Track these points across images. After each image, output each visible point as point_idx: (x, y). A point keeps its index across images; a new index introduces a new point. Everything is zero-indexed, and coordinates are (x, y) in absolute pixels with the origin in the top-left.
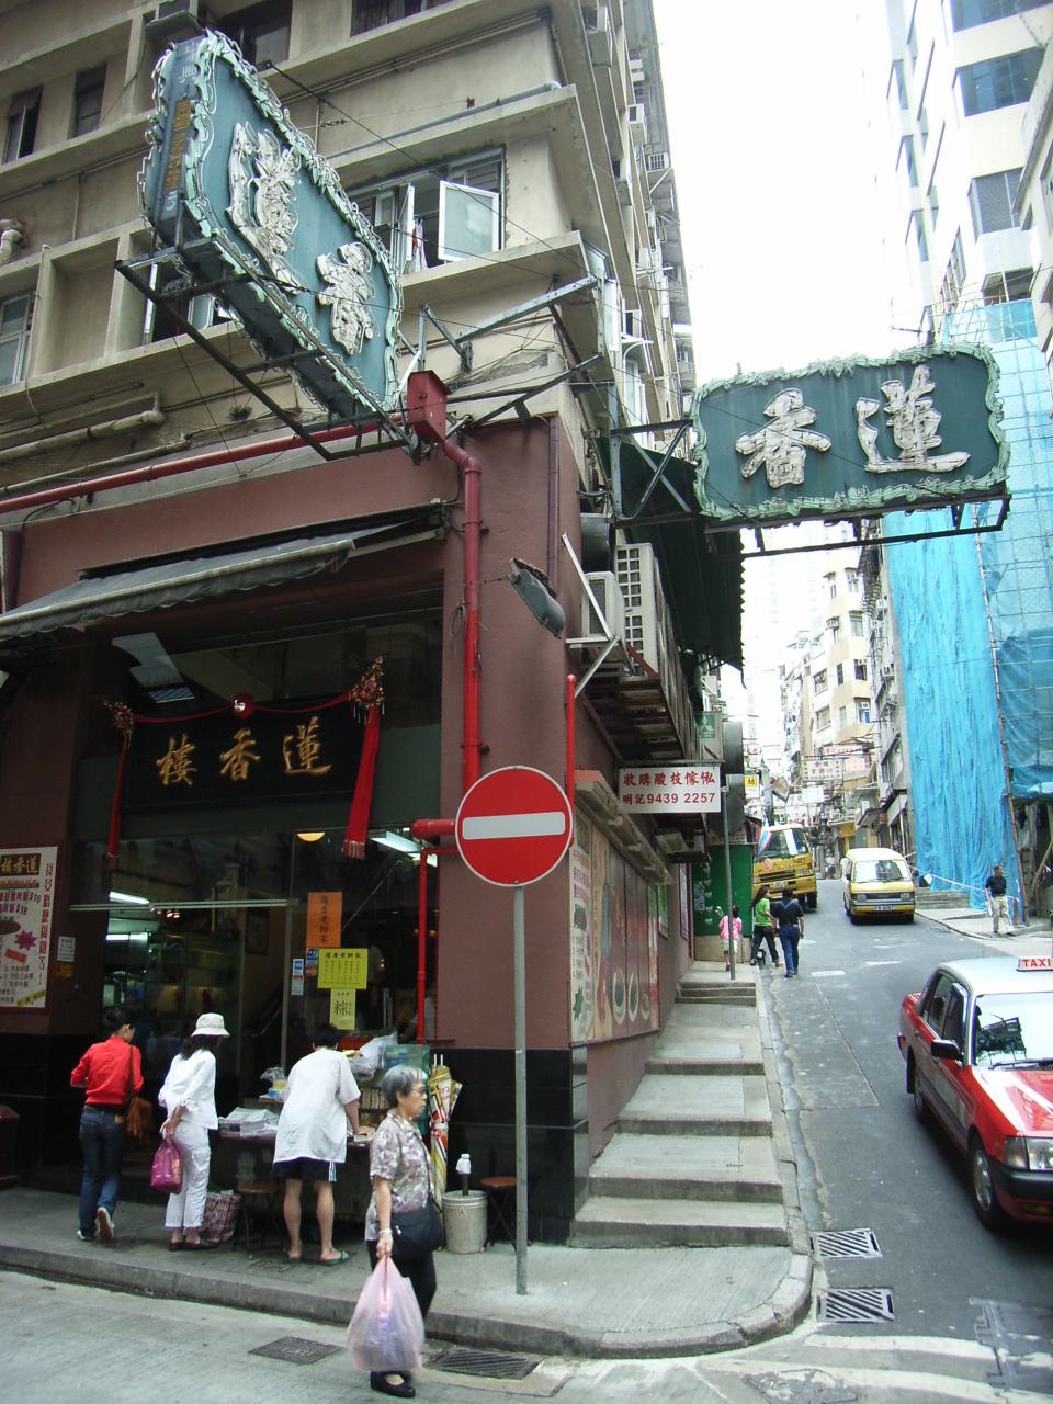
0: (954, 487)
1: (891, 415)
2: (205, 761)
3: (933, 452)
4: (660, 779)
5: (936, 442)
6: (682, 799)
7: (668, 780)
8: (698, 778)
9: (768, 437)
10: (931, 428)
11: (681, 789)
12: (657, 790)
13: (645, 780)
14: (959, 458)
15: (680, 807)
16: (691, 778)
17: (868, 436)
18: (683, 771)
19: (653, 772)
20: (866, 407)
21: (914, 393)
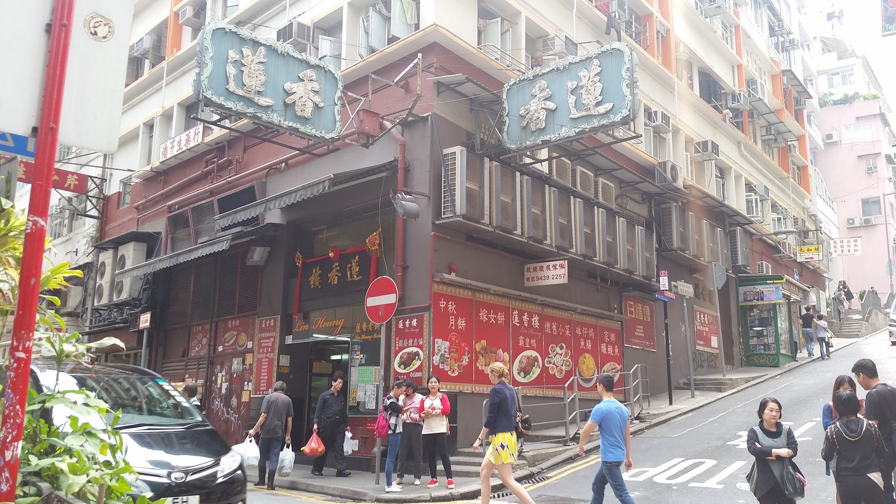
0: (604, 122)
1: (582, 87)
2: (324, 277)
3: (598, 104)
4: (541, 268)
5: (600, 98)
6: (551, 277)
7: (545, 269)
8: (558, 267)
9: (533, 105)
10: (599, 91)
11: (552, 272)
12: (540, 274)
13: (535, 269)
14: (608, 106)
15: (550, 282)
16: (555, 267)
17: (572, 99)
18: (551, 264)
19: (539, 265)
20: (571, 84)
21: (593, 74)
